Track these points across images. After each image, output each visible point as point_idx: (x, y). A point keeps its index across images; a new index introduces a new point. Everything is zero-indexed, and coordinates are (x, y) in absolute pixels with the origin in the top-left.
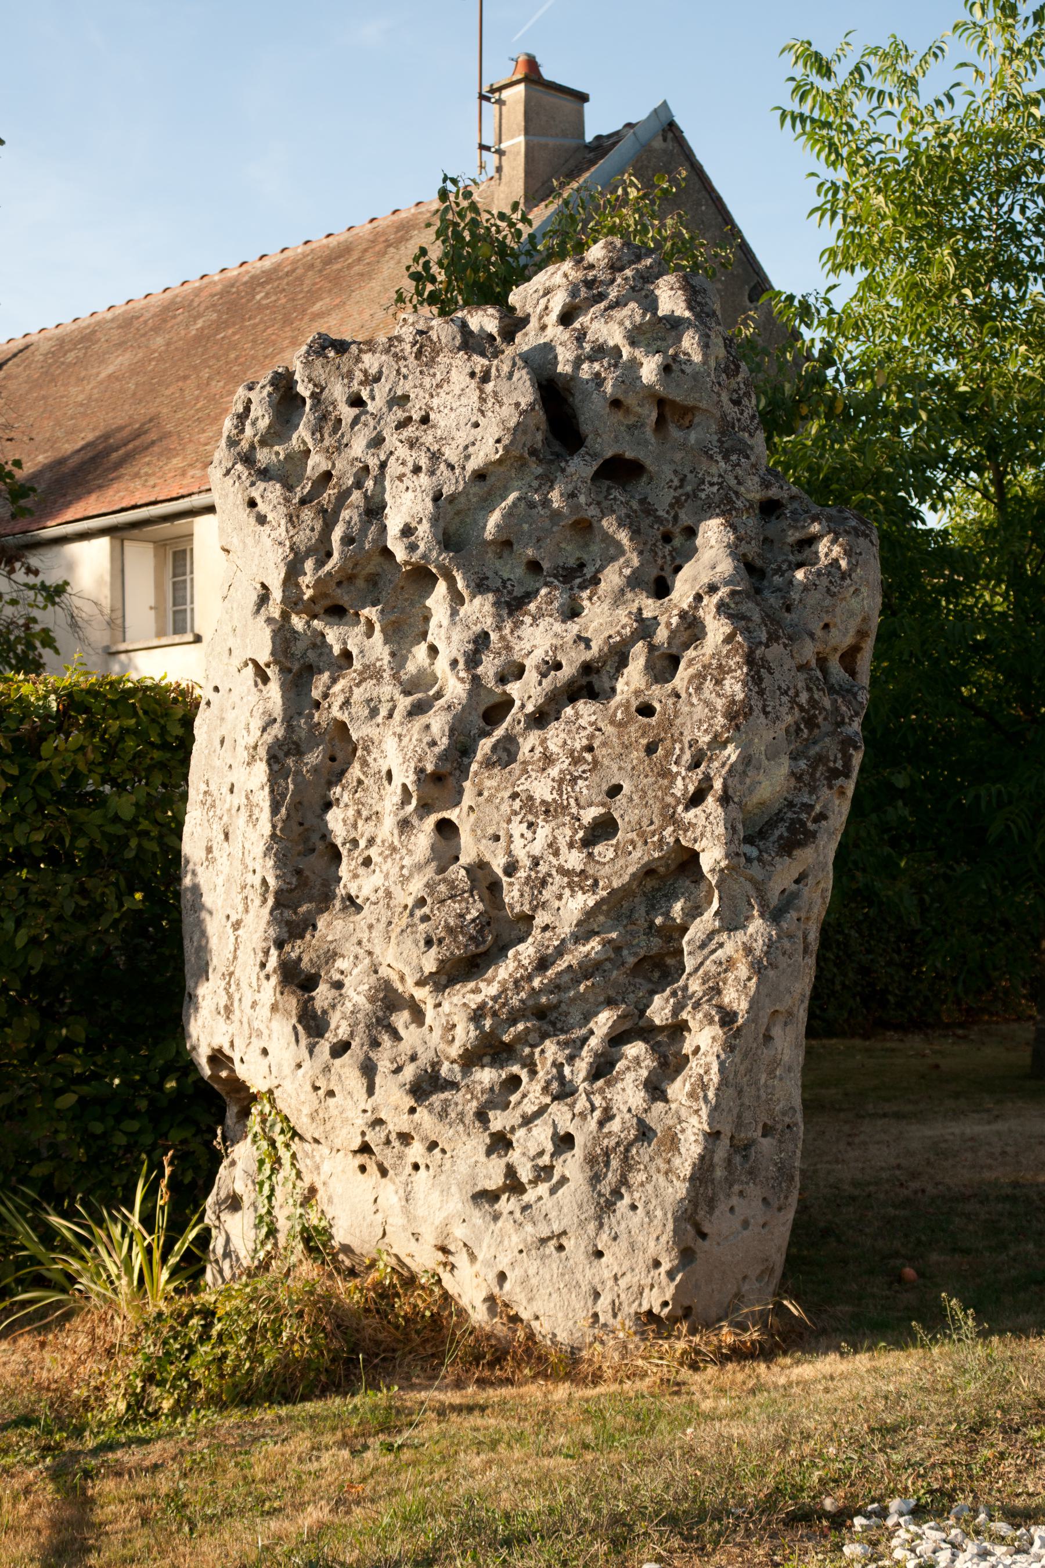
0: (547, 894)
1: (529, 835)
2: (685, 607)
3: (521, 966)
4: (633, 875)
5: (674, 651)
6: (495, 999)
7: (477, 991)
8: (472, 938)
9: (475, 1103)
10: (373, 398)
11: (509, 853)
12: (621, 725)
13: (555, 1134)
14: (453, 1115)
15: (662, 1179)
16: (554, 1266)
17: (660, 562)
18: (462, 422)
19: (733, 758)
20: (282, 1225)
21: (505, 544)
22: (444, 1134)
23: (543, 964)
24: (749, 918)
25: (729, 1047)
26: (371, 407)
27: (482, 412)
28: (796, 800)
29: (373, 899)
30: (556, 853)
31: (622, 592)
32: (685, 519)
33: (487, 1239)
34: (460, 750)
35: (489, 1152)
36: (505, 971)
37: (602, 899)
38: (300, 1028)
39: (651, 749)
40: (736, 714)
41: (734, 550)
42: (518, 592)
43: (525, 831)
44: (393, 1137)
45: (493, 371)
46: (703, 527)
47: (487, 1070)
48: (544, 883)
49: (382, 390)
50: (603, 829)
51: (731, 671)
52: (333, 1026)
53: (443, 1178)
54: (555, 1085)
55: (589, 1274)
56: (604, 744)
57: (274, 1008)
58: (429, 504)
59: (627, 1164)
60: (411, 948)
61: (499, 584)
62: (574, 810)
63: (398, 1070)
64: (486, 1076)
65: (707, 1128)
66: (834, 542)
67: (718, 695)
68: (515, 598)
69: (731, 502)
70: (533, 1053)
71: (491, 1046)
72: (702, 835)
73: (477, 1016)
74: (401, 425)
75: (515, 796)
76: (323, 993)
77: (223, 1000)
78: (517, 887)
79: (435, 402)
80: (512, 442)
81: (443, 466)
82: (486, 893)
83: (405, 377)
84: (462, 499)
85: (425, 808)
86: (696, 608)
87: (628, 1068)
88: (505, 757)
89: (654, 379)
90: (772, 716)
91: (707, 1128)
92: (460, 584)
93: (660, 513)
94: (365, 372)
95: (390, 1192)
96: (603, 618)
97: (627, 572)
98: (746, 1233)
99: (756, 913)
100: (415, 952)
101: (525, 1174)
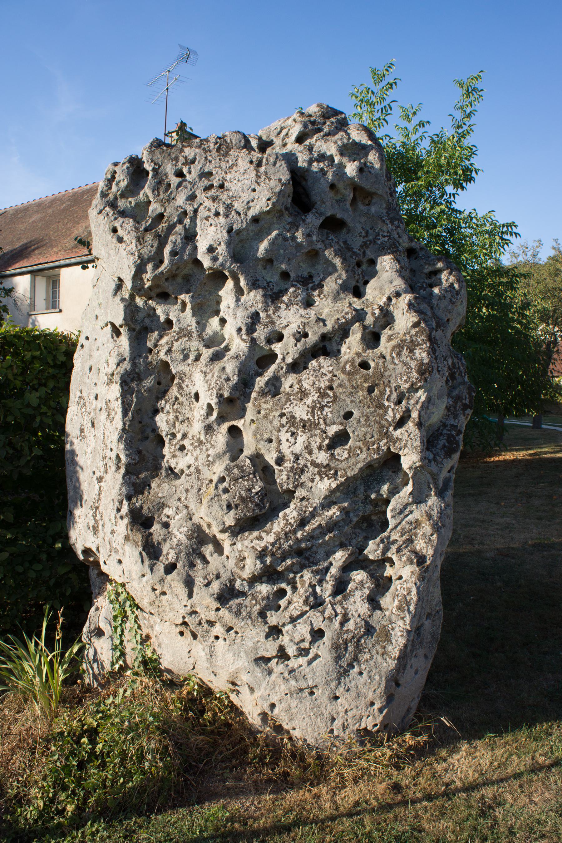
0: (304, 478)
1: (292, 440)
2: (382, 304)
3: (288, 523)
4: (361, 469)
5: (376, 330)
6: (273, 544)
7: (260, 538)
8: (257, 505)
9: (258, 607)
10: (190, 173)
11: (279, 451)
12: (349, 374)
13: (312, 629)
14: (244, 614)
15: (379, 658)
16: (308, 704)
17: (357, 277)
18: (246, 188)
19: (423, 398)
20: (128, 650)
21: (269, 261)
22: (238, 624)
23: (303, 522)
24: (429, 496)
25: (422, 578)
26: (188, 177)
27: (258, 183)
28: (447, 422)
29: (187, 472)
30: (310, 453)
31: (338, 293)
32: (370, 254)
33: (264, 685)
34: (244, 385)
35: (267, 637)
36: (278, 526)
37: (341, 484)
38: (144, 553)
39: (370, 390)
40: (423, 371)
41: (401, 272)
42: (276, 289)
43: (290, 438)
44: (203, 621)
45: (264, 161)
46: (380, 259)
47: (264, 585)
48: (302, 471)
49: (195, 169)
50: (341, 438)
51: (419, 345)
52: (164, 552)
53: (235, 646)
54: (311, 599)
55: (328, 709)
56: (340, 386)
57: (127, 538)
58: (226, 235)
59: (358, 649)
60: (217, 510)
61: (265, 284)
62: (323, 427)
63: (208, 585)
64: (264, 589)
65: (409, 628)
66: (450, 274)
67: (412, 359)
68: (275, 293)
69: (396, 247)
70: (295, 577)
71: (268, 572)
72: (405, 446)
73: (261, 555)
74: (208, 188)
75: (282, 415)
76: (156, 528)
77: (92, 523)
78: (285, 473)
79: (228, 177)
80: (277, 201)
81: (233, 213)
82: (261, 472)
83: (210, 162)
84: (245, 233)
85: (221, 419)
86: (388, 305)
87: (356, 588)
88: (273, 389)
89: (354, 174)
90: (441, 373)
91: (409, 628)
92: (242, 283)
93: (355, 250)
94: (186, 158)
95: (199, 650)
96: (330, 307)
97: (340, 282)
98: (417, 676)
99: (433, 493)
100: (220, 513)
101: (291, 651)
